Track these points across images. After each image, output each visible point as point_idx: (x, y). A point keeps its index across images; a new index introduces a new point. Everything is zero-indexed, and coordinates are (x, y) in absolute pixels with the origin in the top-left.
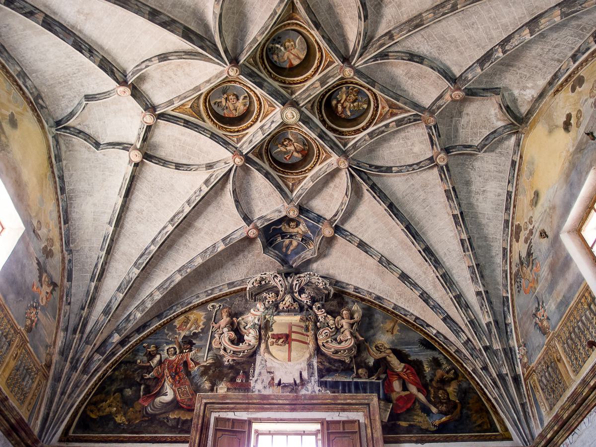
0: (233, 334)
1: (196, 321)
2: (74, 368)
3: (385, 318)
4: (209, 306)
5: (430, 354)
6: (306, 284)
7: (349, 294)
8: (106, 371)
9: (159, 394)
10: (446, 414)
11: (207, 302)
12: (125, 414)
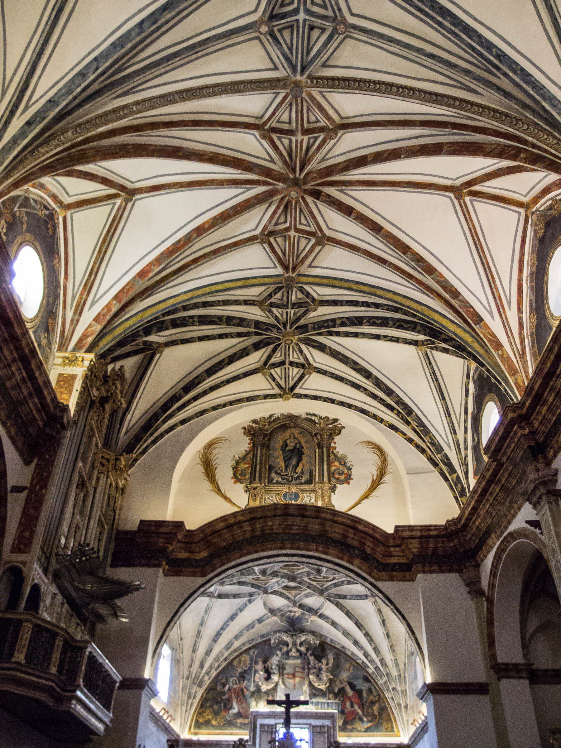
0: (266, 675)
1: (245, 663)
2: (189, 697)
3: (346, 661)
4: (251, 652)
5: (368, 685)
6: (304, 641)
7: (327, 643)
8: (203, 695)
9: (231, 708)
10: (370, 722)
11: (249, 649)
12: (216, 720)
